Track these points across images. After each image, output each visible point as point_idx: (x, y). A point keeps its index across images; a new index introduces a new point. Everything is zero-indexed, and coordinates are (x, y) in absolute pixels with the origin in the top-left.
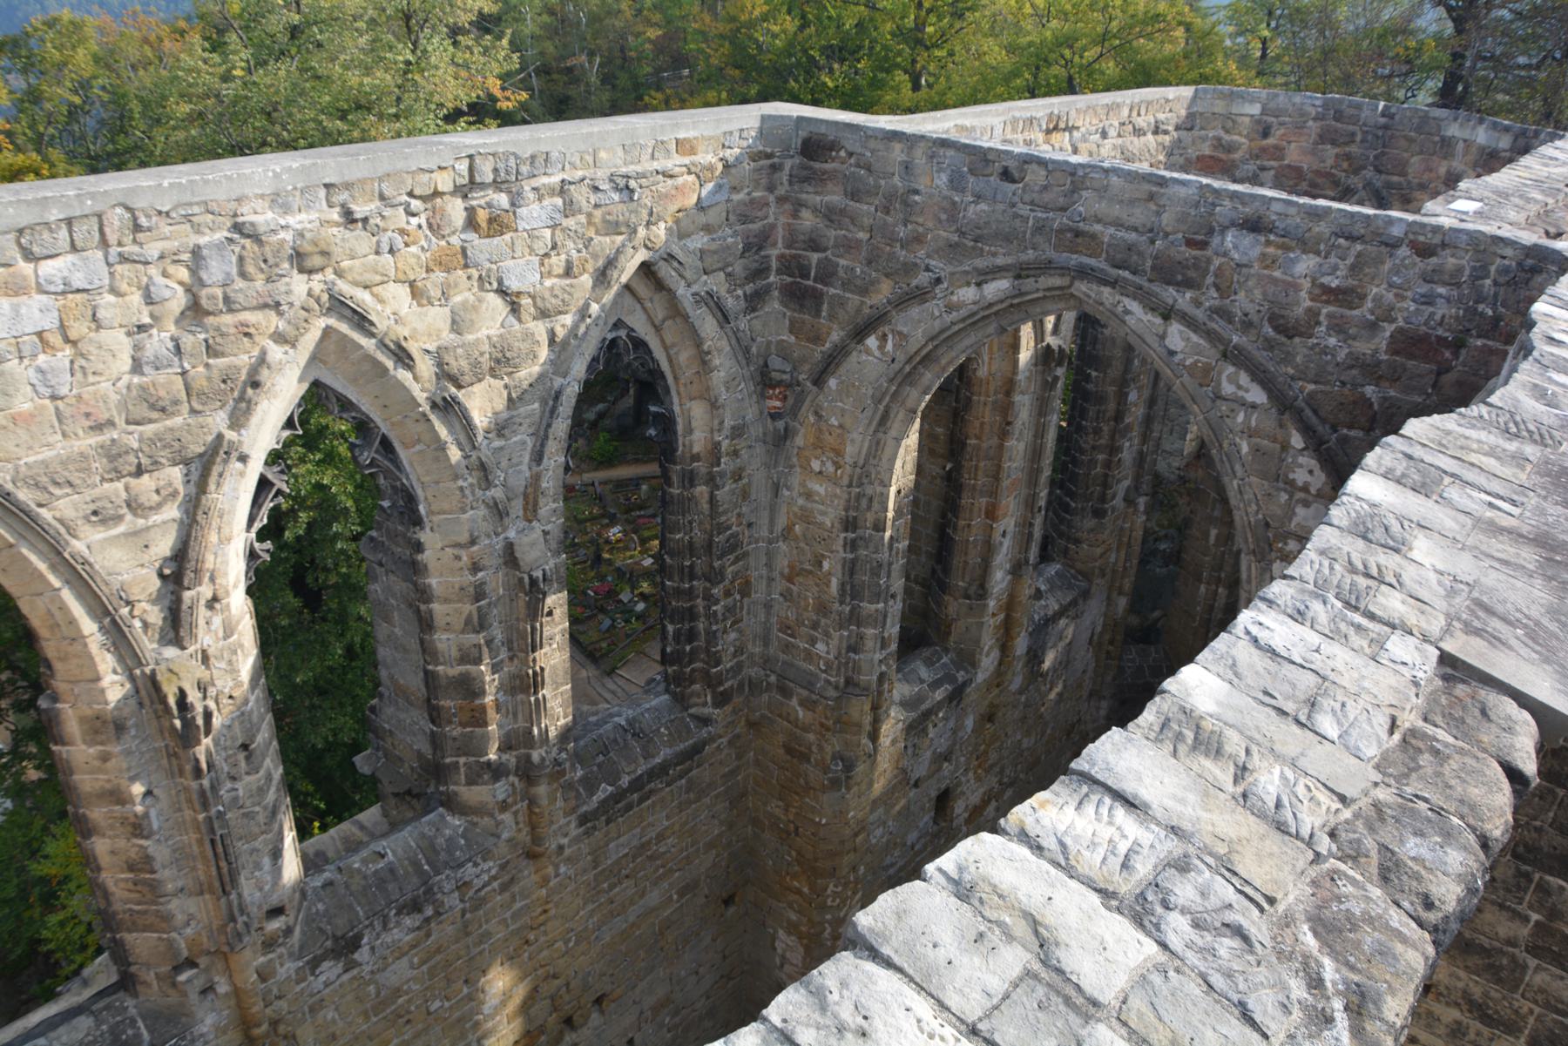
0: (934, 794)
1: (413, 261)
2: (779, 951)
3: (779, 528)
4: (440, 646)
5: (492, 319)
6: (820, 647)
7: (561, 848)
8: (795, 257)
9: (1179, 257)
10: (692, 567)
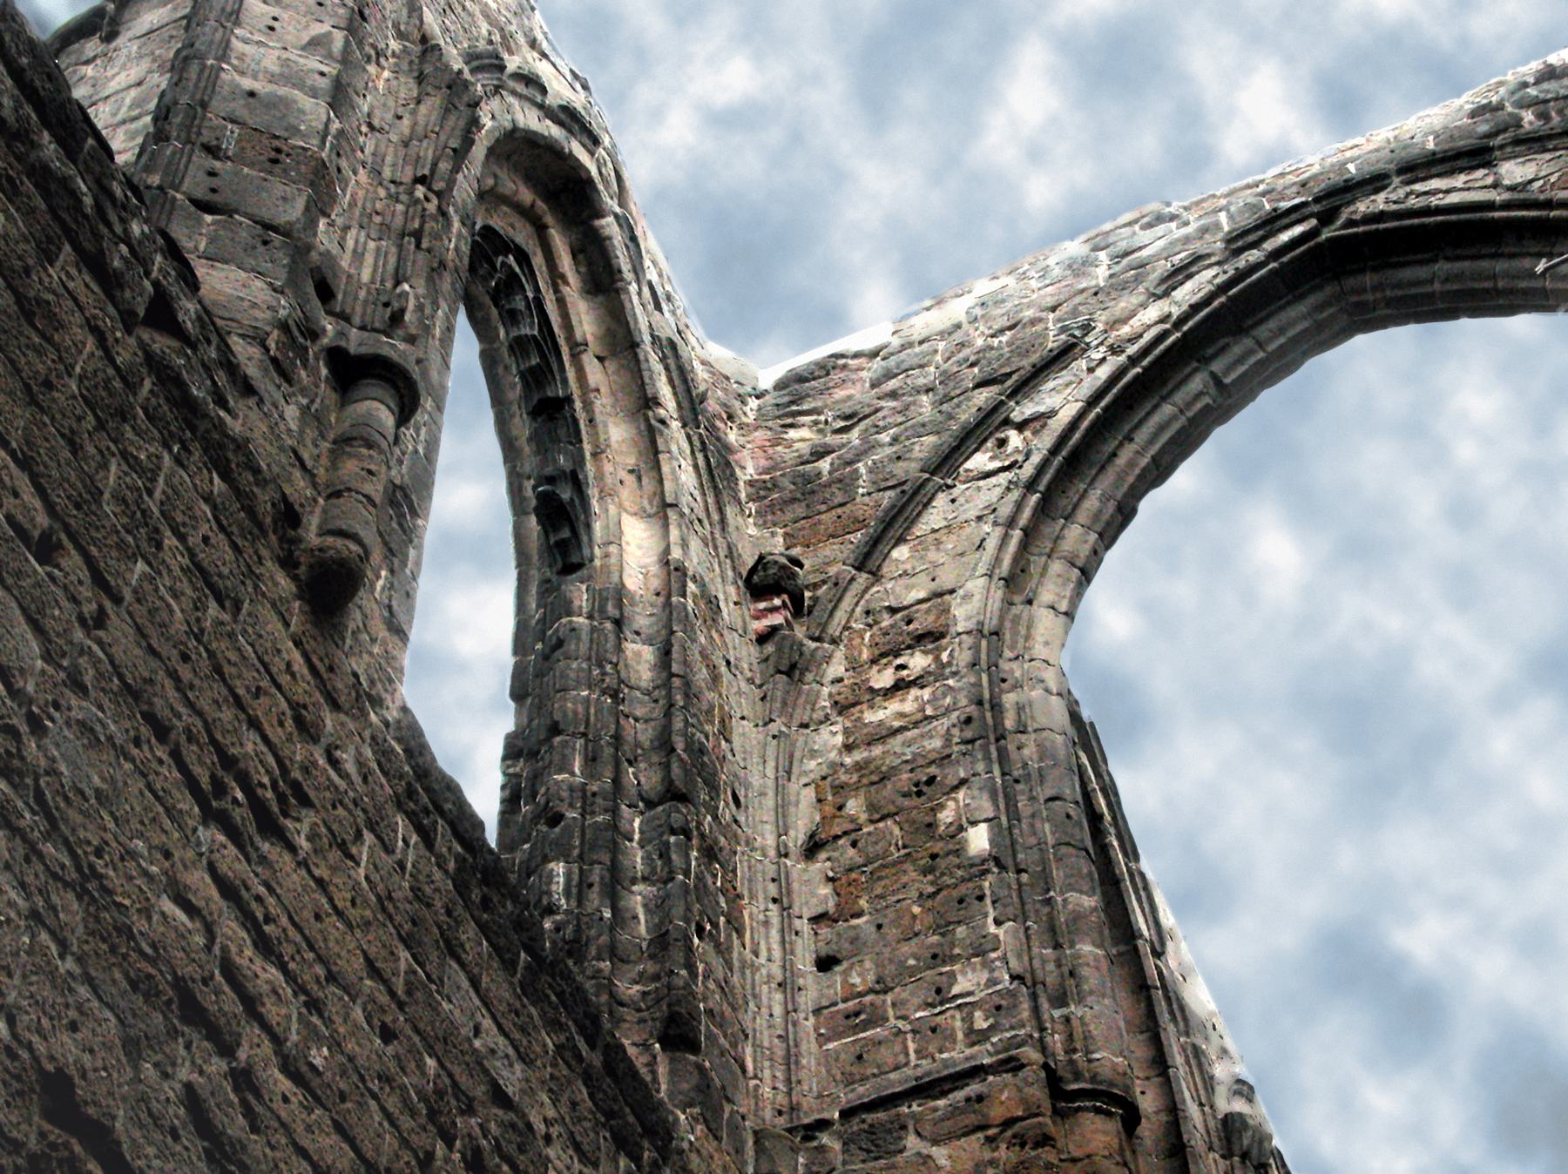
6: (968, 981)
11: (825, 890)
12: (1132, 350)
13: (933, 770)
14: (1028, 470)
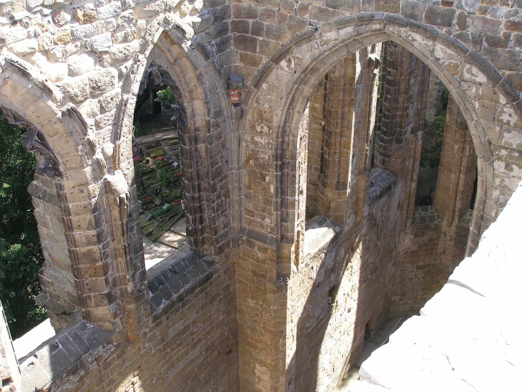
0: (327, 289)
1: (47, 40)
2: (257, 375)
4: (77, 237)
5: (88, 69)
6: (267, 220)
7: (145, 334)
8: (240, 22)
9: (439, 11)
10: (199, 185)
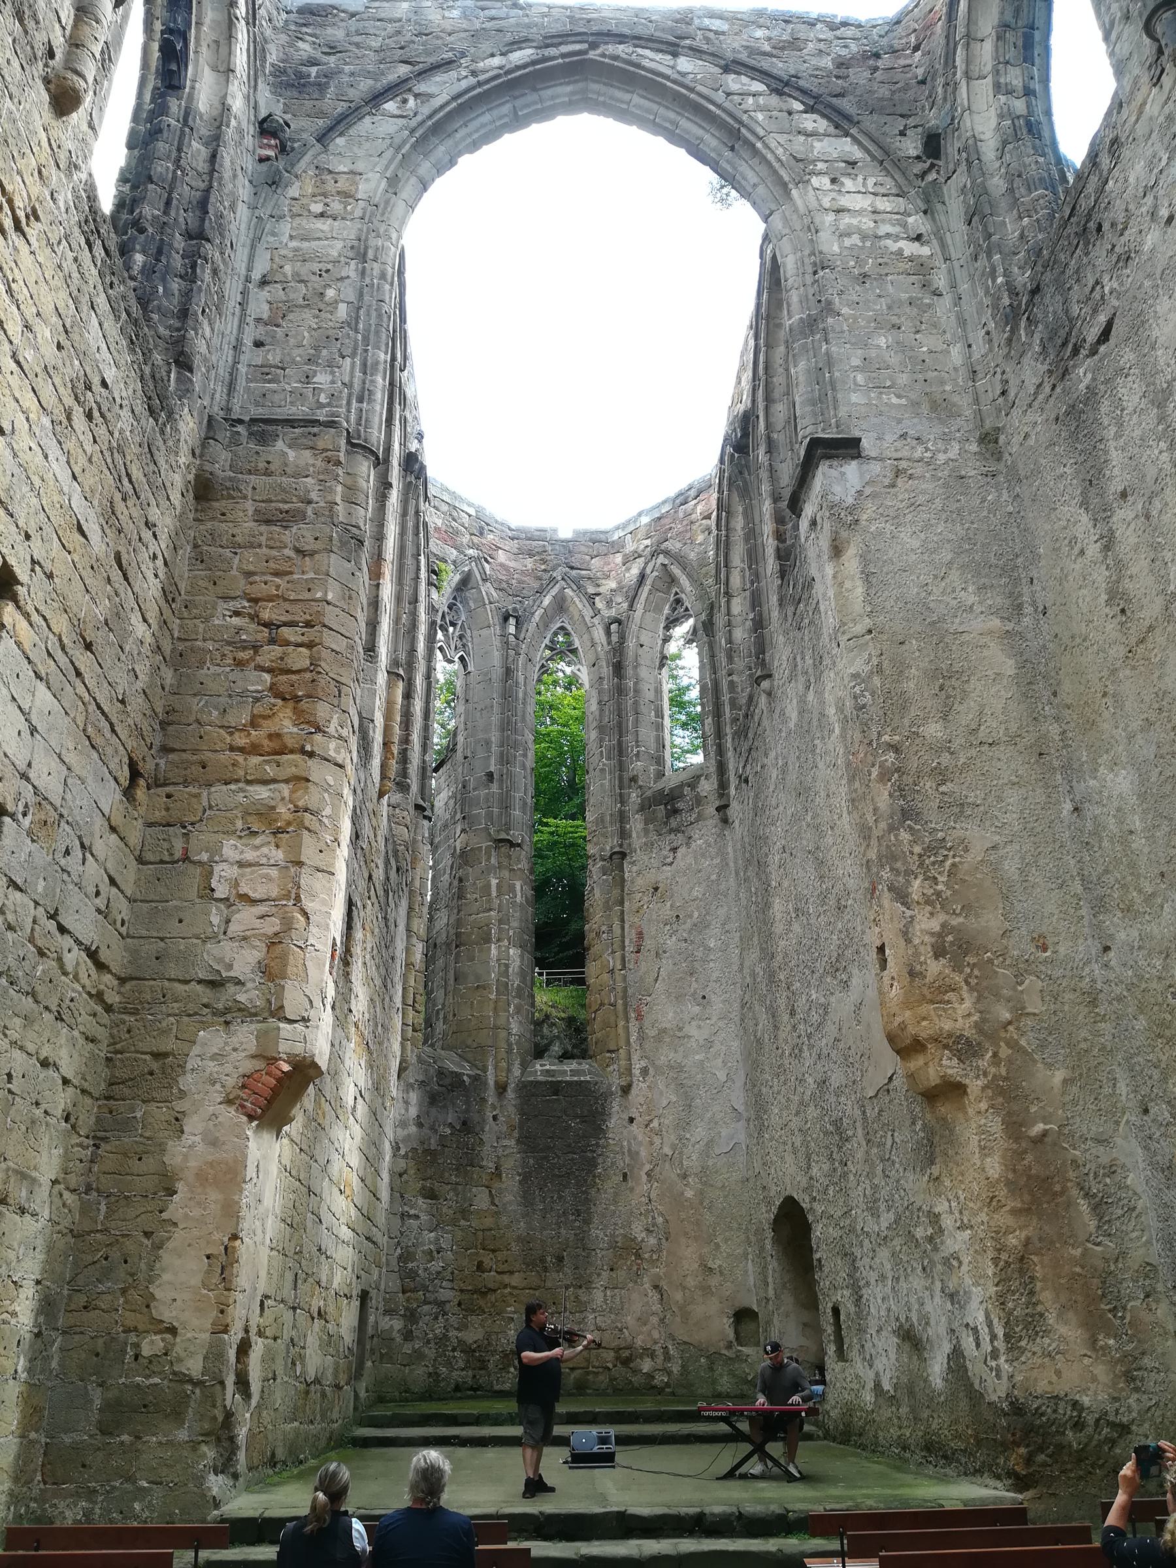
3: (256, 275)
6: (322, 378)
11: (266, 307)
12: (482, 78)
13: (329, 266)
14: (413, 123)
